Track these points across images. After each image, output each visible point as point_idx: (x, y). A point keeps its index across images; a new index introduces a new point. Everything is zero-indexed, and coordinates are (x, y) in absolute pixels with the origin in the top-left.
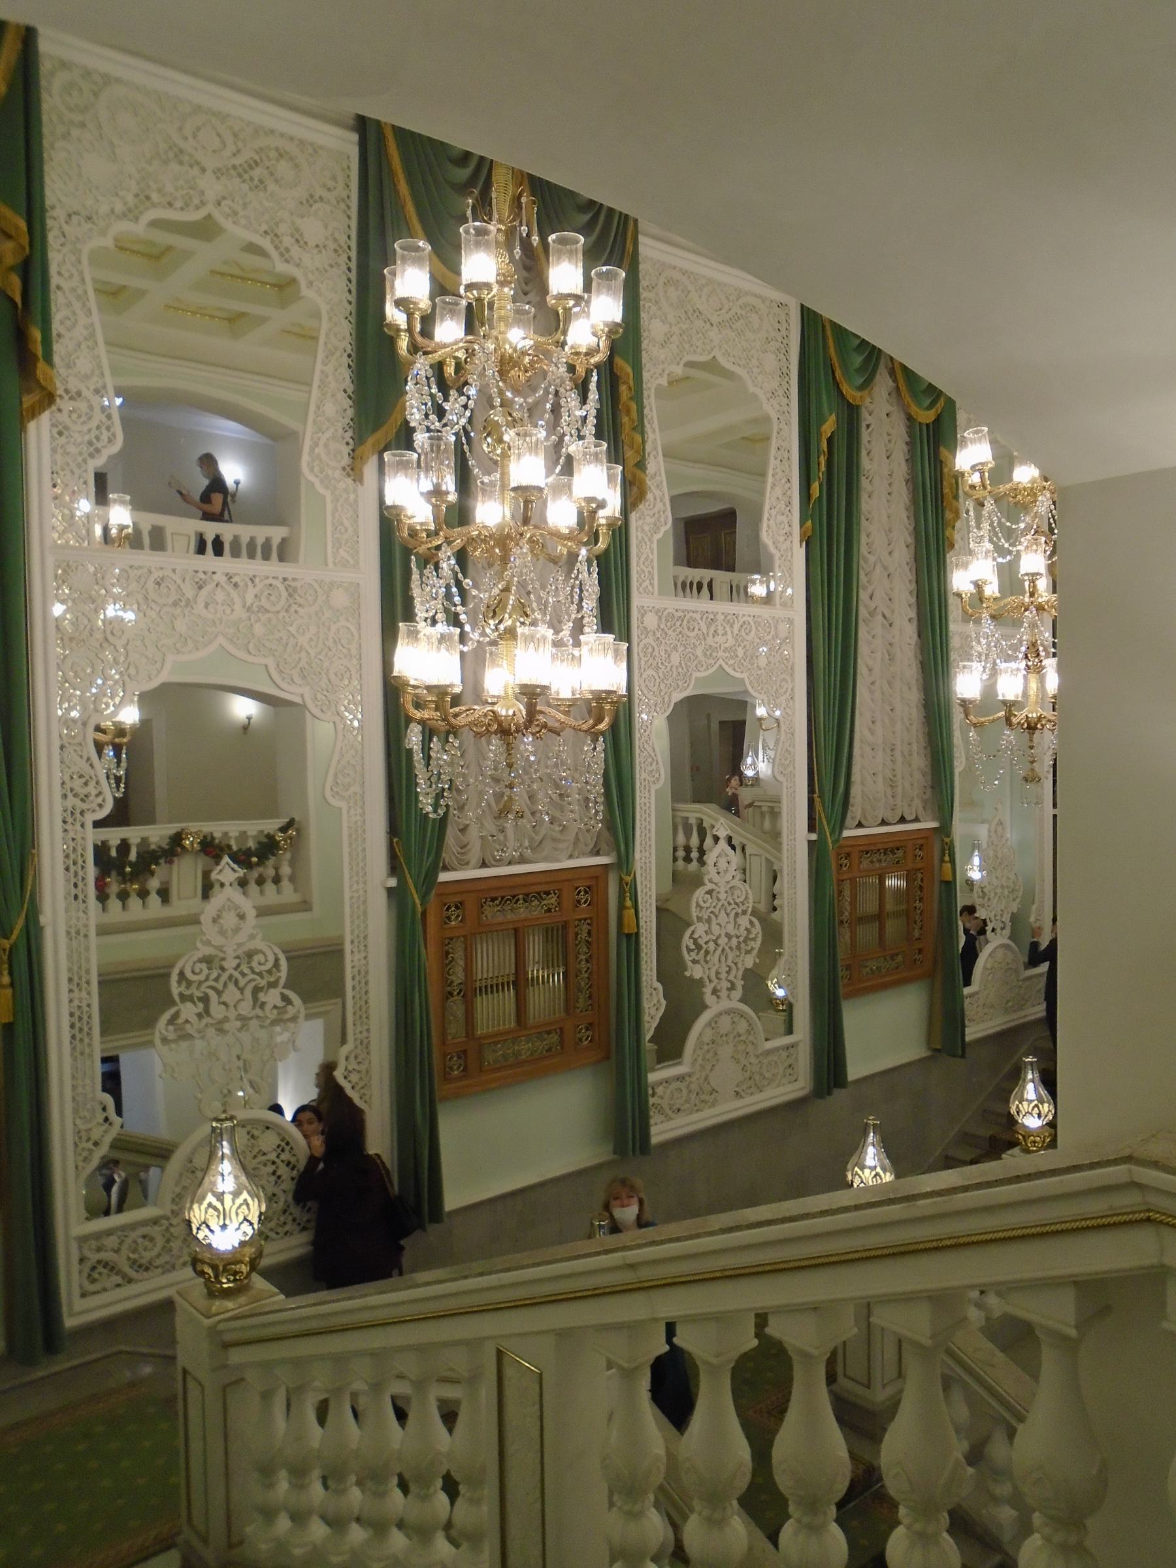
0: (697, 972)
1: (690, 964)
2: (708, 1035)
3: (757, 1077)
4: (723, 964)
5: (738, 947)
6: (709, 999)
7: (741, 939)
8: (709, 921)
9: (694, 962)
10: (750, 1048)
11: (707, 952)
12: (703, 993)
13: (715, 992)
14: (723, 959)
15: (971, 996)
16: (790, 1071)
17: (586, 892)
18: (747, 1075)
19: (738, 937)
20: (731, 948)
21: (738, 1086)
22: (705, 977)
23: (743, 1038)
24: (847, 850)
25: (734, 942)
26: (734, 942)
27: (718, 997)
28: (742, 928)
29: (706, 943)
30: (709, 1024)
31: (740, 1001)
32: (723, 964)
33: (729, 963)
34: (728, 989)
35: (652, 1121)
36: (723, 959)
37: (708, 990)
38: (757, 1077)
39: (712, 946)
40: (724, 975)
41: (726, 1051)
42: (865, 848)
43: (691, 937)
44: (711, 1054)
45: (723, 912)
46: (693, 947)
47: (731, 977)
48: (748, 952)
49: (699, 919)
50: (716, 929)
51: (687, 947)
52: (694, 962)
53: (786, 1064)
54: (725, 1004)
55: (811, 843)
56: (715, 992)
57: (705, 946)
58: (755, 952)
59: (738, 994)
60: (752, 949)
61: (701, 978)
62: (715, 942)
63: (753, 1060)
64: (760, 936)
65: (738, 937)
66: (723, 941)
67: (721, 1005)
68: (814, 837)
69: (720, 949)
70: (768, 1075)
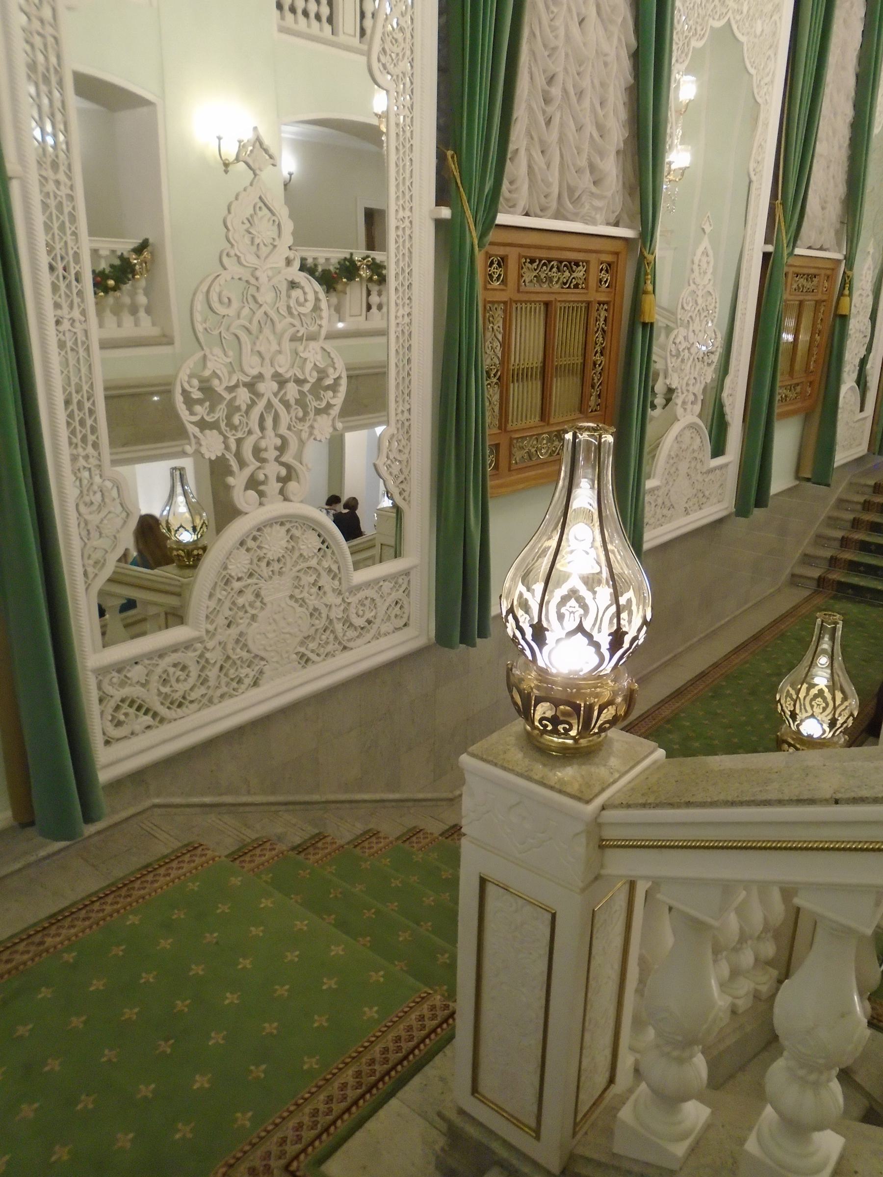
1: (192, 429)
2: (240, 564)
3: (339, 627)
4: (270, 432)
5: (301, 402)
7: (306, 387)
9: (203, 425)
10: (325, 581)
11: (232, 408)
14: (269, 422)
15: (653, 490)
18: (320, 624)
19: (299, 382)
20: (287, 405)
21: (302, 643)
24: (501, 251)
25: (292, 391)
26: (292, 391)
27: (261, 494)
28: (309, 366)
29: (231, 389)
32: (270, 432)
33: (283, 430)
36: (269, 422)
38: (339, 627)
39: (243, 396)
41: (277, 591)
42: (533, 253)
44: (249, 596)
45: (267, 331)
46: (197, 395)
47: (287, 458)
48: (318, 412)
51: (184, 392)
52: (203, 425)
53: (390, 600)
54: (275, 508)
55: (440, 224)
56: (253, 484)
57: (228, 396)
60: (329, 406)
62: (251, 386)
63: (332, 598)
64: (344, 382)
65: (299, 382)
66: (268, 387)
68: (445, 213)
69: (261, 405)
70: (359, 622)
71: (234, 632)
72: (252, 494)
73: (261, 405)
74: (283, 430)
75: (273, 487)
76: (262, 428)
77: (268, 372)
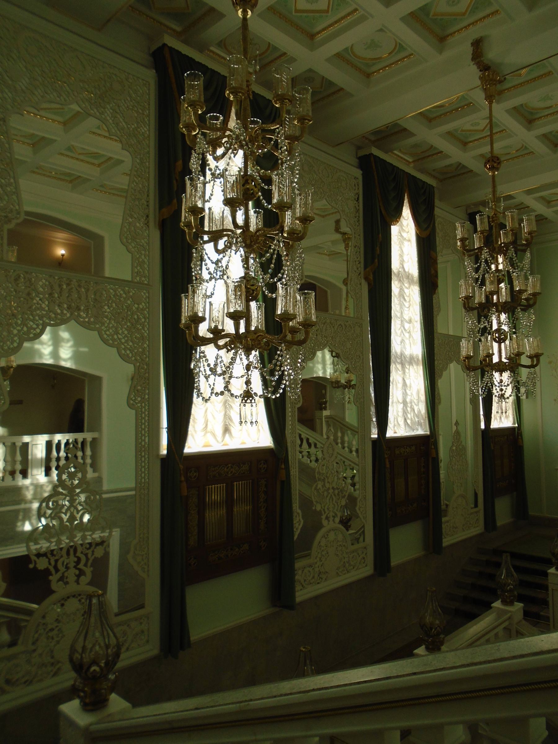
0: (318, 508)
1: (315, 503)
5: (338, 494)
6: (325, 522)
8: (324, 480)
12: (322, 518)
13: (327, 518)
15: (447, 522)
16: (363, 561)
17: (264, 464)
20: (335, 495)
21: (337, 569)
22: (322, 510)
23: (341, 543)
26: (336, 492)
29: (323, 492)
30: (323, 536)
31: (339, 523)
34: (334, 517)
35: (297, 589)
37: (324, 517)
40: (331, 509)
43: (316, 489)
48: (343, 497)
49: (319, 480)
50: (327, 485)
56: (327, 518)
58: (346, 497)
59: (337, 520)
61: (320, 511)
66: (331, 491)
67: (330, 525)
69: (329, 496)
71: (321, 563)
72: (326, 521)
73: (329, 496)
74: (334, 502)
75: (331, 519)
76: (330, 502)
77: (331, 487)
